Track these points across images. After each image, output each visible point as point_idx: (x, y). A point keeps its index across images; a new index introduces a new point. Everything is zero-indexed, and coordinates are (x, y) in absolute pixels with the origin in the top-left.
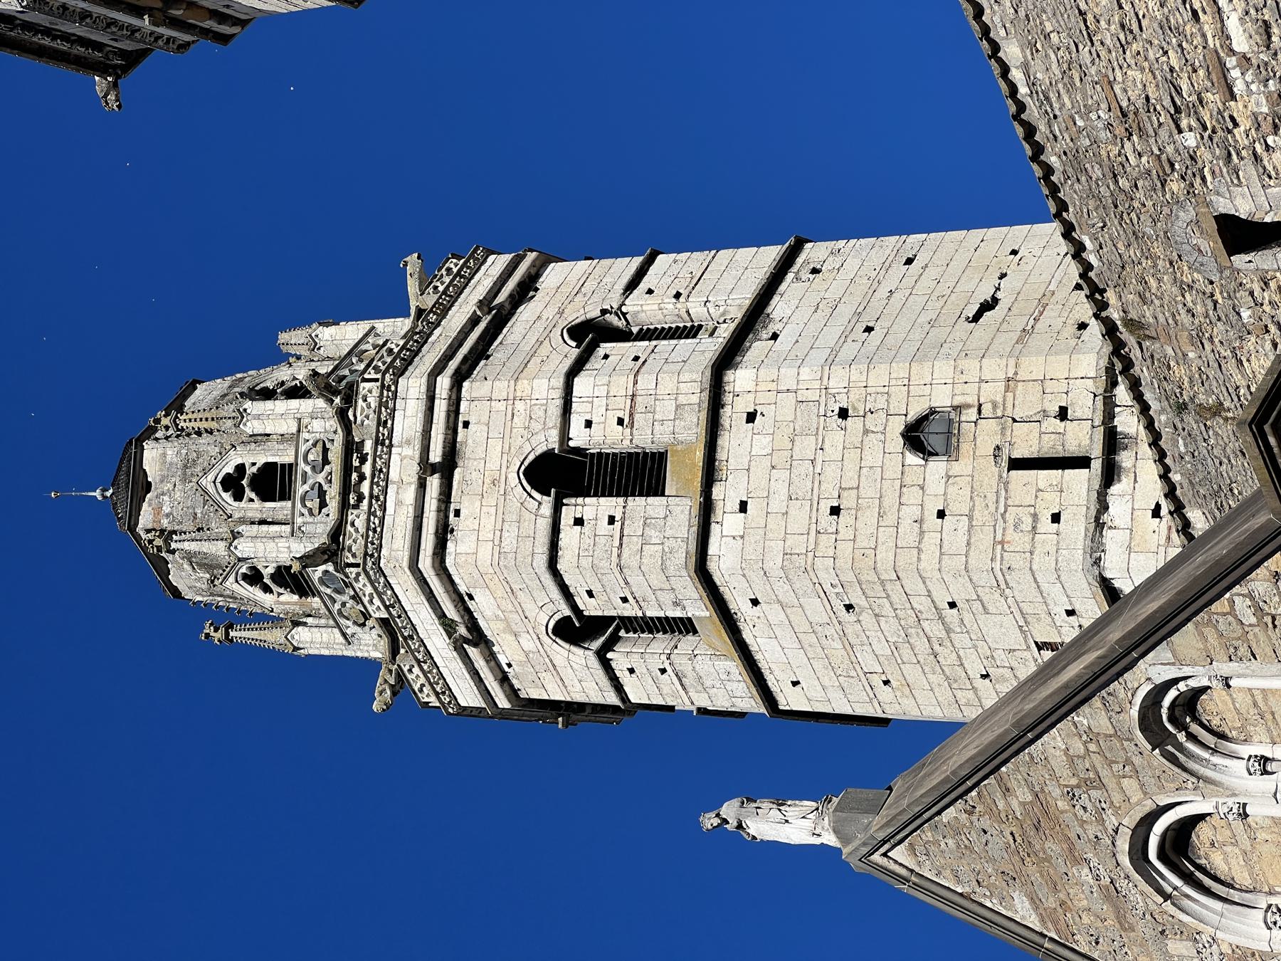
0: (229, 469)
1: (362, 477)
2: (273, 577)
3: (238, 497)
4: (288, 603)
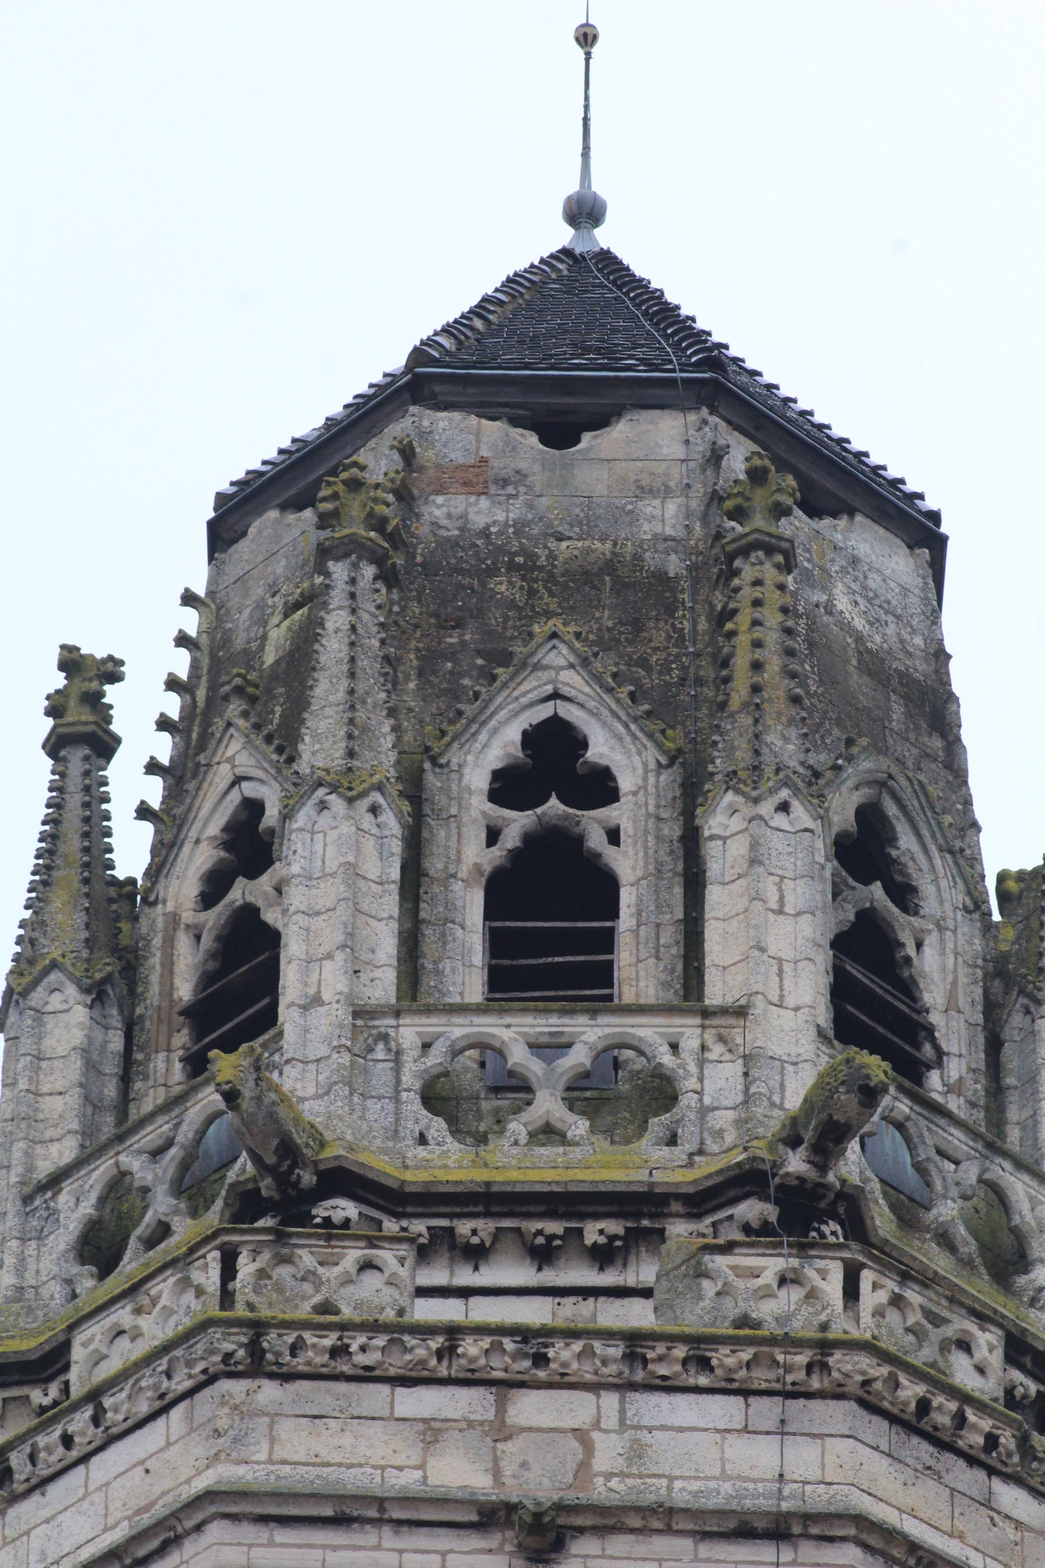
0: (603, 747)
1: (543, 1254)
2: (248, 914)
3: (509, 787)
4: (169, 964)
